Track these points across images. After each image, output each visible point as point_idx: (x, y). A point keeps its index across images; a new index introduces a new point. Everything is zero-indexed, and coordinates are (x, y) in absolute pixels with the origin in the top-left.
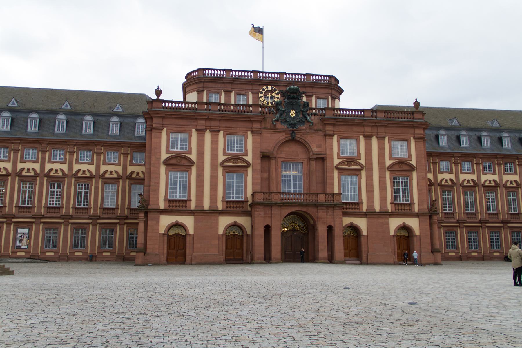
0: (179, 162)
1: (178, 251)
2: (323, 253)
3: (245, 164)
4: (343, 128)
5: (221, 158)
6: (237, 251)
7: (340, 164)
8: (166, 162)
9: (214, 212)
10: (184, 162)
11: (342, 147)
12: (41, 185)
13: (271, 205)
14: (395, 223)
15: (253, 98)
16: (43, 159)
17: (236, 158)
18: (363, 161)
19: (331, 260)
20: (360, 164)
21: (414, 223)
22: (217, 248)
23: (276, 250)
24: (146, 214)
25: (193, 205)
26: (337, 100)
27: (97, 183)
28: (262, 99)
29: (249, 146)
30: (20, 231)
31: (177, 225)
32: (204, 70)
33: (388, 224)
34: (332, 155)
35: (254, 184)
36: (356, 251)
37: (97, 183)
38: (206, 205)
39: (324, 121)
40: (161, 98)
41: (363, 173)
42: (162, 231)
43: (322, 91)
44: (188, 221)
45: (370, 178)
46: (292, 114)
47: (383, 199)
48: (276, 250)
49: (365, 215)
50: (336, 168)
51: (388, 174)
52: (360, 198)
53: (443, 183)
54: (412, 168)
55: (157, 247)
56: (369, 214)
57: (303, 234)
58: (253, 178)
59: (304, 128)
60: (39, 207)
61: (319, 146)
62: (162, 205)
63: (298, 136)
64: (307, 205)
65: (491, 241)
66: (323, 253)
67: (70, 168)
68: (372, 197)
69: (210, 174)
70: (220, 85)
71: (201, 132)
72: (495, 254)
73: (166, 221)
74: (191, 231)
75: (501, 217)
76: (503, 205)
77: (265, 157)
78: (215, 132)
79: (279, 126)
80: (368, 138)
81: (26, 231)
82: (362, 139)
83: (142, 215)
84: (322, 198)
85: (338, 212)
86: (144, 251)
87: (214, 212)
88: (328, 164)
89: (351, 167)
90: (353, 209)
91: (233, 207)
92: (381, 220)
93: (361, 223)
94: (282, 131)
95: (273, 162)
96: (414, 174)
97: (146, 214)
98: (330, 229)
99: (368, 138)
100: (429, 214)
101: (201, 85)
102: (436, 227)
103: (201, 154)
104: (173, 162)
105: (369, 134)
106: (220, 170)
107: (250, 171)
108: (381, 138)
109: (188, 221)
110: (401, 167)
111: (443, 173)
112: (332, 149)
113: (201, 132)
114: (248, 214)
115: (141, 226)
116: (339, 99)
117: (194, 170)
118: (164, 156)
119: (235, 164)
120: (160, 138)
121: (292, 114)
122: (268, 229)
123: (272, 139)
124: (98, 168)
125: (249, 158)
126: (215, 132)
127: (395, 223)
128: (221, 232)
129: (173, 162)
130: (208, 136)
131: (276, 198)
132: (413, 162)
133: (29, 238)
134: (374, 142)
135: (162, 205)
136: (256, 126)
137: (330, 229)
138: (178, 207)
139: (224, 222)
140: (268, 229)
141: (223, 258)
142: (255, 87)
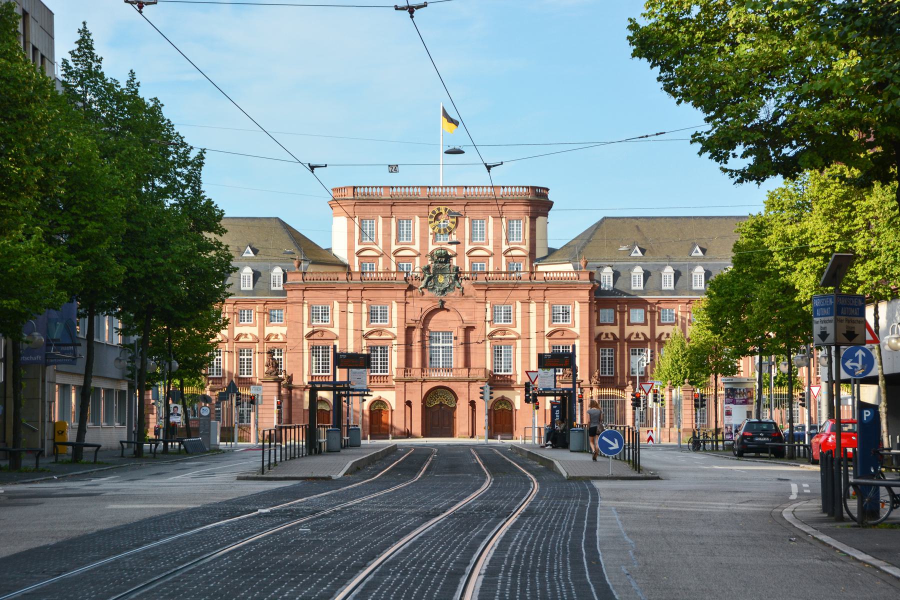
3: (389, 337)
8: (308, 336)
15: (421, 223)
18: (518, 330)
26: (540, 220)
53: (663, 339)
59: (453, 294)
64: (448, 381)
94: (431, 299)
103: (344, 328)
114: (391, 387)
116: (546, 215)
118: (307, 330)
121: (441, 279)
132: (577, 330)
134: (533, 307)
137: (472, 404)
140: (409, 403)
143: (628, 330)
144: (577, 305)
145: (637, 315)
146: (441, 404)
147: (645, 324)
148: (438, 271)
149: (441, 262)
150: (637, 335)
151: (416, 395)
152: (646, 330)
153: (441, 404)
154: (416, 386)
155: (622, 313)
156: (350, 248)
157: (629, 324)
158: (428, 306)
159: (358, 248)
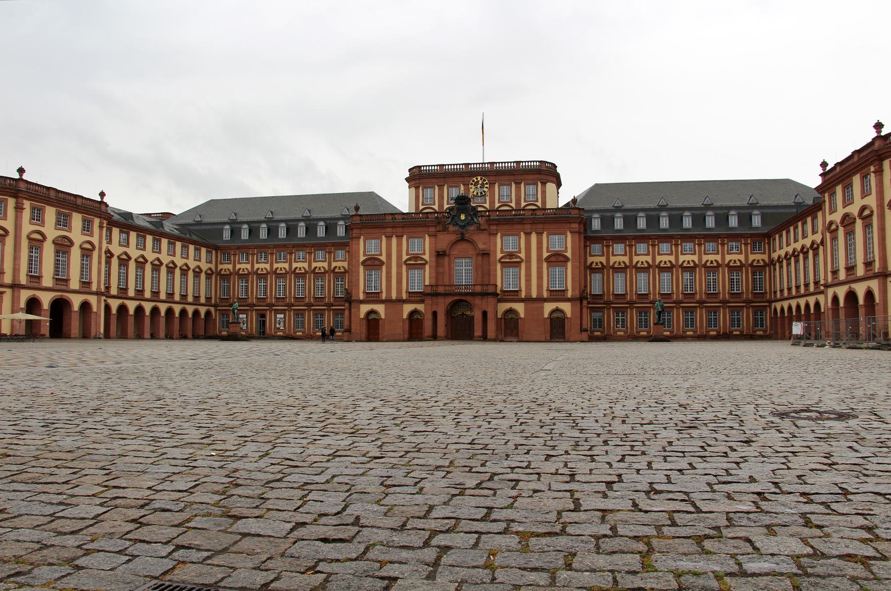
0: (373, 263)
1: (373, 331)
2: (478, 332)
4: (506, 227)
5: (405, 257)
6: (415, 331)
7: (502, 258)
8: (364, 263)
9: (400, 301)
10: (377, 263)
11: (502, 244)
12: (290, 280)
13: (436, 295)
14: (548, 307)
16: (291, 259)
17: (416, 257)
18: (522, 255)
19: (484, 338)
20: (520, 257)
21: (566, 307)
22: (402, 328)
23: (441, 331)
24: (350, 303)
25: (384, 296)
27: (329, 277)
28: (472, 190)
29: (425, 246)
30: (279, 316)
31: (372, 312)
32: (420, 167)
33: (543, 308)
34: (496, 251)
35: (430, 278)
36: (510, 330)
37: (329, 277)
38: (394, 296)
39: (490, 222)
40: (361, 212)
41: (523, 265)
42: (362, 316)
43: (531, 177)
44: (380, 308)
45: (528, 269)
46: (463, 217)
47: (540, 287)
48: (441, 331)
49: (522, 300)
50: (500, 262)
51: (545, 265)
52: (520, 287)
53: (639, 265)
54: (567, 259)
55: (359, 328)
56: (528, 300)
57: (458, 317)
58: (430, 273)
60: (290, 297)
61: (485, 244)
62: (362, 297)
63: (467, 236)
65: (755, 320)
66: (478, 332)
67: (310, 265)
68: (530, 285)
69: (399, 271)
70: (434, 180)
71: (389, 238)
72: (688, 333)
73: (364, 309)
74: (383, 317)
75: (698, 297)
76: (701, 285)
77: (440, 255)
78: (400, 237)
79: (451, 228)
80: (528, 234)
81: (282, 316)
82: (522, 234)
83: (347, 305)
84: (478, 289)
85: (491, 300)
86: (349, 330)
87: (400, 301)
88: (492, 258)
89: (511, 261)
90: (513, 296)
91: (413, 297)
92: (536, 305)
93: (520, 308)
94: (454, 232)
95: (446, 259)
96: (569, 265)
97: (350, 303)
98: (485, 314)
99: (528, 234)
100: (582, 298)
101: (417, 181)
102: (585, 310)
103: (389, 256)
104: (369, 263)
105: (529, 231)
106: (404, 267)
107: (427, 267)
108: (539, 234)
109: (380, 308)
110: (557, 259)
111: (639, 255)
112: (496, 246)
113: (389, 238)
115: (347, 312)
117: (384, 268)
118: (362, 258)
119: (415, 263)
120: (359, 245)
121: (463, 217)
122: (435, 314)
123: (445, 240)
124: (330, 264)
125: (426, 257)
126: (400, 237)
127: (548, 307)
128: (405, 316)
129: (369, 263)
130: (394, 240)
131: (441, 290)
132: (569, 254)
133: (285, 323)
134: (534, 237)
135: (362, 297)
136: (432, 229)
137: (485, 314)
138: (373, 297)
139: (408, 308)
140: (435, 314)
141: (406, 336)
142: (467, 179)
143: (613, 259)
144: (569, 235)
145: (619, 248)
146: (463, 314)
147: (625, 255)
148: (460, 211)
149: (462, 204)
150: (619, 263)
151: (441, 307)
152: (626, 259)
153: (463, 314)
154: (441, 300)
155: (608, 246)
156: (417, 207)
157: (613, 255)
158: (453, 237)
159: (421, 207)
